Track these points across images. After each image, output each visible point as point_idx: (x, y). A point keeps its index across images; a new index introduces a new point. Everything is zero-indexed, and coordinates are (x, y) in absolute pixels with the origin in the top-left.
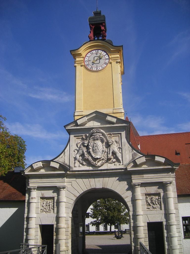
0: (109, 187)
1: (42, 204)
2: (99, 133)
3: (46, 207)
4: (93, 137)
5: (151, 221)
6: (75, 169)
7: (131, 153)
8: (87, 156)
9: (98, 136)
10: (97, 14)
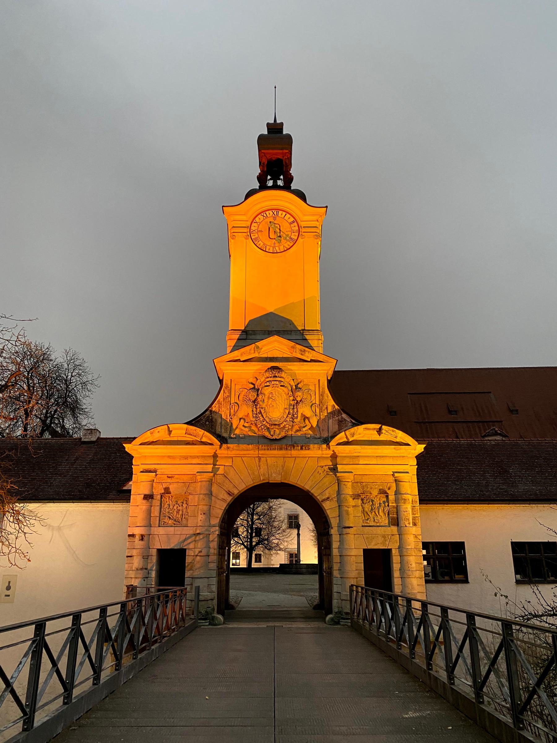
7: (337, 418)
9: (277, 383)
10: (275, 129)
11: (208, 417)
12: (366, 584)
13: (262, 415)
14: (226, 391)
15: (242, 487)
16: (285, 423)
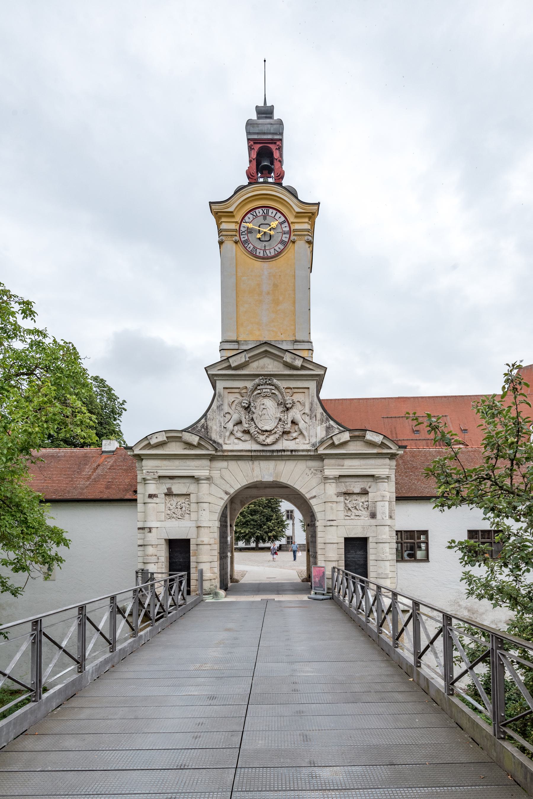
1: (169, 505)
2: (269, 384)
3: (176, 510)
4: (259, 391)
6: (225, 447)
7: (325, 425)
8: (247, 425)
9: (269, 390)
11: (203, 425)
12: (347, 566)
13: (254, 423)
14: (219, 400)
15: (237, 486)
16: (276, 430)
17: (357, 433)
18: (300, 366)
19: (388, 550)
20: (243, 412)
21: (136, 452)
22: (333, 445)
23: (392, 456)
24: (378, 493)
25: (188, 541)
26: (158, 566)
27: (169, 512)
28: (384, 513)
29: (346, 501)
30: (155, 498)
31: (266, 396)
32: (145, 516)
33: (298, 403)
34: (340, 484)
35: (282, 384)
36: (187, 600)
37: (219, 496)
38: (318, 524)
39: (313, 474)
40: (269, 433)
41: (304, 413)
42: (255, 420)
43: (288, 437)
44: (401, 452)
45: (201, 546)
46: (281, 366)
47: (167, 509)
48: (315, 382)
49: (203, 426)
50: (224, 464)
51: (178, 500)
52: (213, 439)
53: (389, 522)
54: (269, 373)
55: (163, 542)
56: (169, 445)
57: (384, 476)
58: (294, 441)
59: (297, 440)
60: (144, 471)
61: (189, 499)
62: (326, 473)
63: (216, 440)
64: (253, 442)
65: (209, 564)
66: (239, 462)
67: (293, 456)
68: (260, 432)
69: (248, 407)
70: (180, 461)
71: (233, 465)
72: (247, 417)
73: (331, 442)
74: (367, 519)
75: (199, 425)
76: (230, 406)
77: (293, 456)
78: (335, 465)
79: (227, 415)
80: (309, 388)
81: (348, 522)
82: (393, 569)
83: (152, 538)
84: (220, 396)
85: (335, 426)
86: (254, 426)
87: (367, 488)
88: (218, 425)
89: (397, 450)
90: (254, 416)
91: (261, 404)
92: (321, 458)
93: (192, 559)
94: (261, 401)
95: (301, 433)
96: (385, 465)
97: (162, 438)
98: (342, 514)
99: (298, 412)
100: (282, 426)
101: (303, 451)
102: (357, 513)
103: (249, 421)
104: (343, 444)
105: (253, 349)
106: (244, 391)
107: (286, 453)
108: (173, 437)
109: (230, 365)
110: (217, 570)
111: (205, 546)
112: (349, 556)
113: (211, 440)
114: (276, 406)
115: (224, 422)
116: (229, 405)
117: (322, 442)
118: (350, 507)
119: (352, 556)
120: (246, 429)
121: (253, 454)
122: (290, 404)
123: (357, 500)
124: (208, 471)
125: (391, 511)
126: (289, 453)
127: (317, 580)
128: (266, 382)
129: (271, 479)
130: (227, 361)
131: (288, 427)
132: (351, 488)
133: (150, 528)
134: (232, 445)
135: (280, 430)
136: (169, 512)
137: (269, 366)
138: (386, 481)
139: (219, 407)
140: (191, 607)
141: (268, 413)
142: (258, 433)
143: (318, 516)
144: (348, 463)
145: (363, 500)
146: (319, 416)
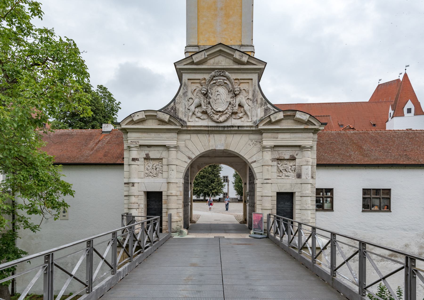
0: (233, 148)
1: (147, 166)
2: (223, 76)
3: (152, 170)
4: (215, 81)
5: (281, 191)
6: (189, 124)
7: (264, 108)
8: (205, 108)
9: (222, 81)
11: (173, 107)
12: (278, 213)
14: (185, 88)
15: (197, 153)
16: (227, 111)
17: (289, 113)
18: (246, 61)
19: (310, 202)
20: (202, 97)
21: (122, 127)
22: (270, 123)
23: (315, 131)
24: (304, 159)
25: (161, 193)
26: (139, 212)
27: (147, 172)
28: (307, 174)
29: (278, 165)
30: (137, 161)
31: (220, 85)
32: (130, 174)
33: (244, 91)
34: (274, 152)
35: (233, 76)
36: (160, 237)
37: (184, 160)
38: (257, 182)
39: (254, 145)
40: (221, 113)
41: (248, 99)
42: (211, 103)
43: (236, 116)
44: (322, 128)
45: (170, 197)
46: (231, 62)
47: (145, 169)
48: (257, 74)
49: (172, 108)
50: (187, 136)
51: (154, 163)
52: (180, 118)
53: (311, 181)
54: (222, 67)
55: (143, 193)
56: (147, 122)
57: (309, 146)
58: (240, 120)
59: (242, 119)
60: (129, 141)
61: (162, 162)
62: (264, 144)
63: (182, 118)
64: (210, 120)
65: (176, 210)
66: (199, 135)
67: (239, 130)
68: (215, 112)
69: (206, 93)
70: (155, 134)
71: (194, 137)
72: (205, 101)
73: (269, 120)
74: (294, 178)
75: (170, 107)
76: (193, 93)
77: (239, 130)
78: (271, 138)
79: (190, 100)
80: (252, 79)
81: (279, 181)
82: (313, 216)
83: (135, 190)
84: (185, 85)
85: (272, 108)
86: (211, 108)
87: (295, 156)
88: (184, 107)
89: (320, 126)
90: (211, 100)
91: (216, 91)
92: (260, 132)
93: (164, 206)
94: (215, 88)
95: (246, 114)
96: (309, 138)
97: (142, 116)
98: (275, 175)
99: (244, 98)
100: (231, 108)
101: (247, 127)
102: (287, 174)
103: (206, 104)
104: (278, 122)
105: (211, 49)
106: (203, 81)
107: (234, 129)
108: (150, 115)
109: (193, 61)
110: (181, 215)
111: (173, 197)
112: (279, 206)
113: (178, 118)
114: (227, 93)
115: (188, 105)
116: (192, 92)
117: (261, 120)
118: (281, 169)
119: (282, 206)
120: (204, 110)
121: (209, 129)
122: (238, 91)
123: (286, 164)
124: (176, 142)
125: (313, 173)
126: (236, 128)
127: (256, 223)
128: (220, 74)
129: (222, 148)
130: (191, 58)
131: (236, 108)
132: (283, 155)
133: (133, 183)
134: (194, 122)
135: (230, 111)
136: (147, 172)
137: (222, 62)
138: (310, 150)
139: (185, 94)
140: (163, 243)
141: (221, 98)
142: (213, 113)
143: (257, 176)
144: (281, 136)
145: (291, 164)
146: (259, 101)
